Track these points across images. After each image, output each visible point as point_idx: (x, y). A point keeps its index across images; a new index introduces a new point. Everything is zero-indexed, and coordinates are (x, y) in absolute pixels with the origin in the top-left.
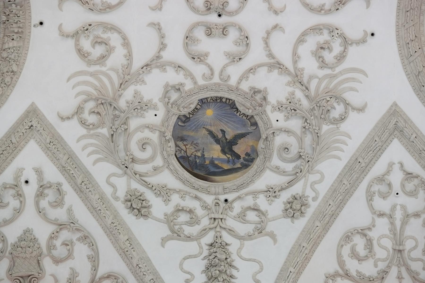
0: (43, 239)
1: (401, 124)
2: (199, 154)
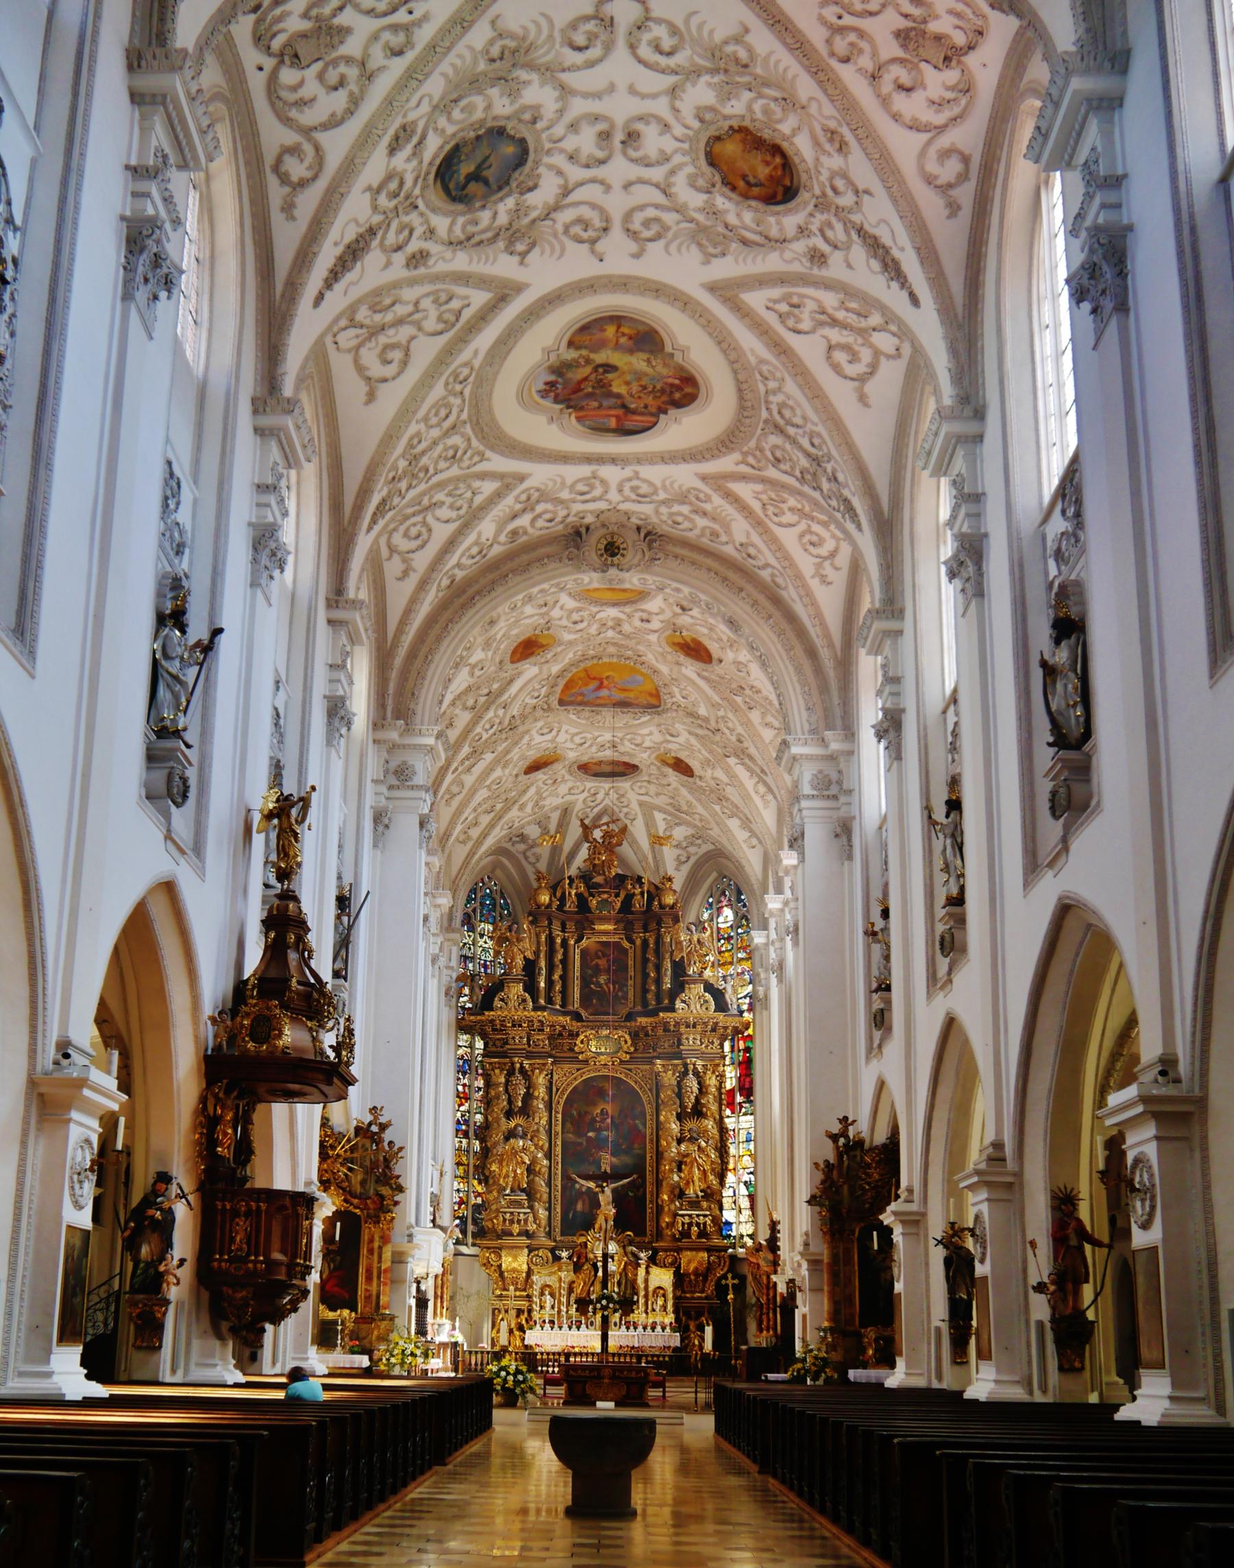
0: (344, 50)
1: (508, 299)
2: (463, 157)
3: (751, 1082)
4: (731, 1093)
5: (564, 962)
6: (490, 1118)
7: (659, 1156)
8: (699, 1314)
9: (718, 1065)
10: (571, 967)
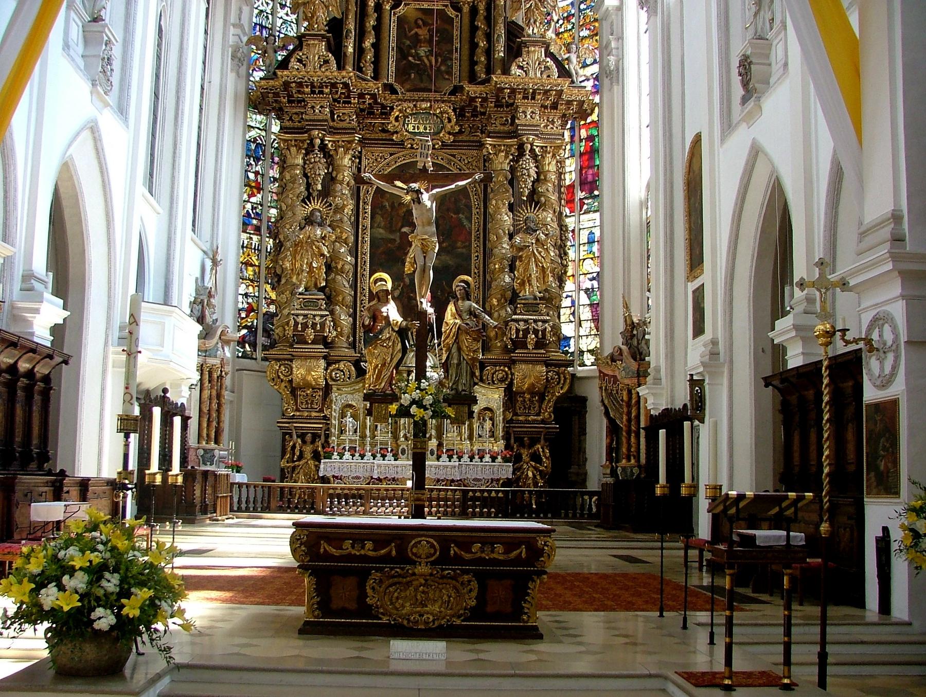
3: (597, 175)
4: (571, 187)
5: (378, 29)
6: (284, 208)
7: (487, 254)
8: (534, 441)
9: (559, 147)
10: (386, 35)
